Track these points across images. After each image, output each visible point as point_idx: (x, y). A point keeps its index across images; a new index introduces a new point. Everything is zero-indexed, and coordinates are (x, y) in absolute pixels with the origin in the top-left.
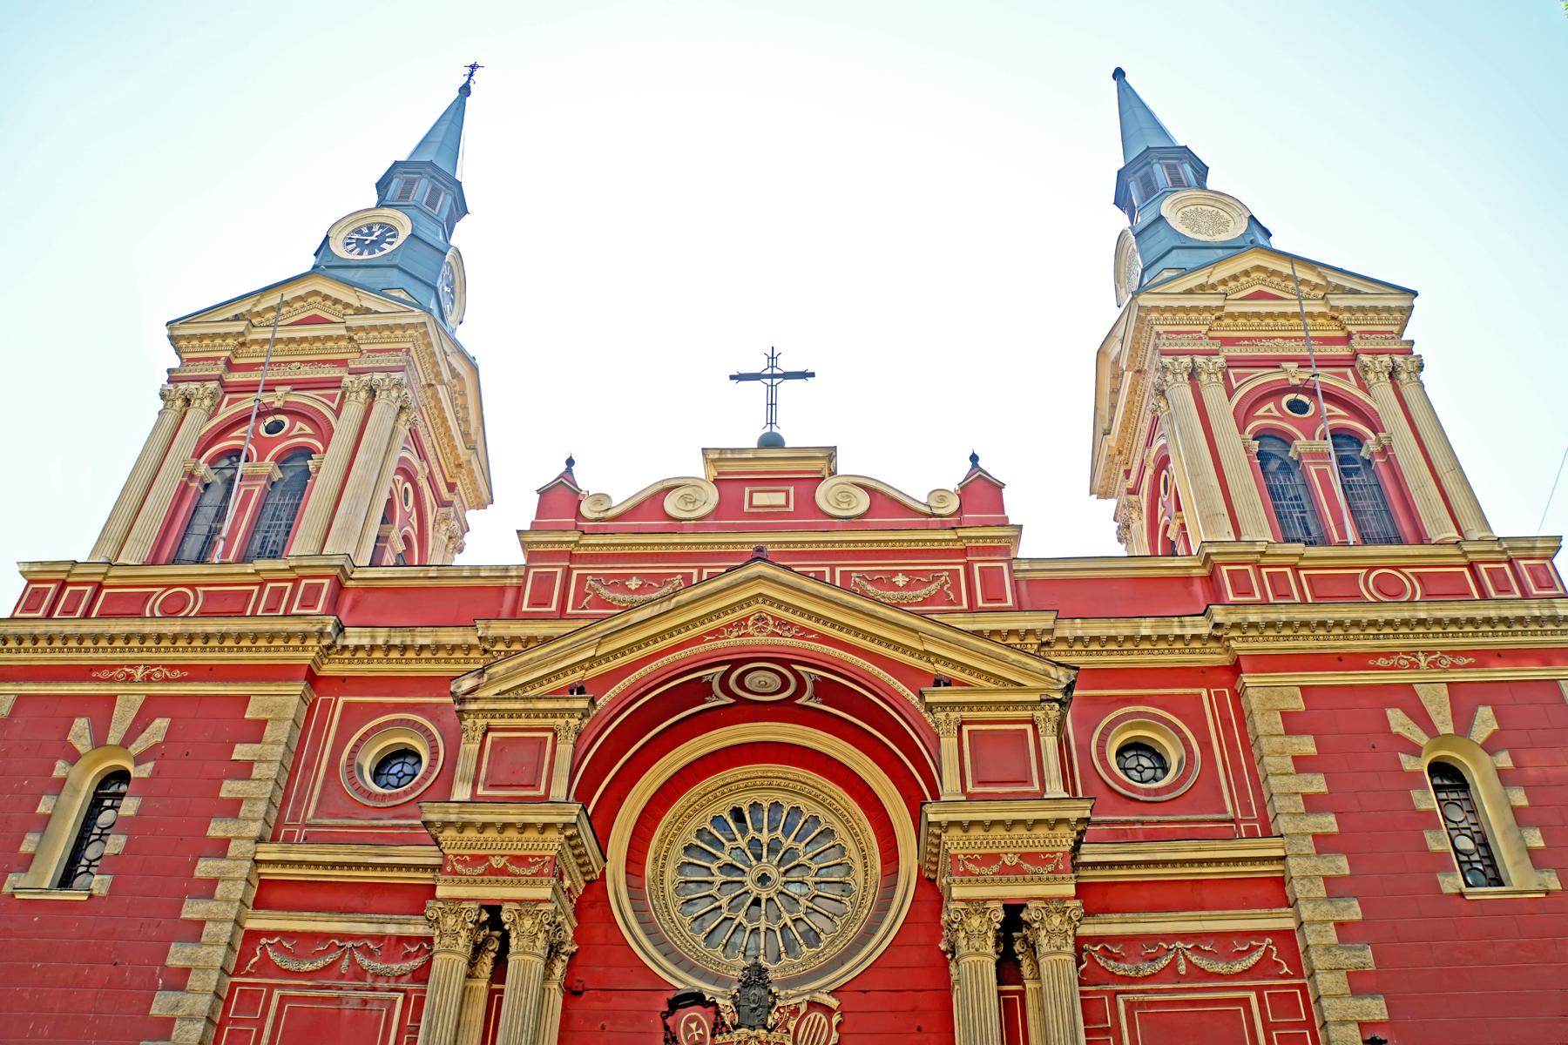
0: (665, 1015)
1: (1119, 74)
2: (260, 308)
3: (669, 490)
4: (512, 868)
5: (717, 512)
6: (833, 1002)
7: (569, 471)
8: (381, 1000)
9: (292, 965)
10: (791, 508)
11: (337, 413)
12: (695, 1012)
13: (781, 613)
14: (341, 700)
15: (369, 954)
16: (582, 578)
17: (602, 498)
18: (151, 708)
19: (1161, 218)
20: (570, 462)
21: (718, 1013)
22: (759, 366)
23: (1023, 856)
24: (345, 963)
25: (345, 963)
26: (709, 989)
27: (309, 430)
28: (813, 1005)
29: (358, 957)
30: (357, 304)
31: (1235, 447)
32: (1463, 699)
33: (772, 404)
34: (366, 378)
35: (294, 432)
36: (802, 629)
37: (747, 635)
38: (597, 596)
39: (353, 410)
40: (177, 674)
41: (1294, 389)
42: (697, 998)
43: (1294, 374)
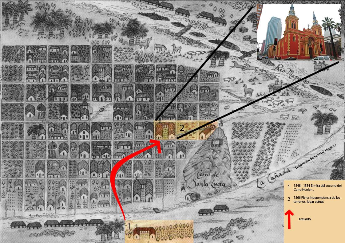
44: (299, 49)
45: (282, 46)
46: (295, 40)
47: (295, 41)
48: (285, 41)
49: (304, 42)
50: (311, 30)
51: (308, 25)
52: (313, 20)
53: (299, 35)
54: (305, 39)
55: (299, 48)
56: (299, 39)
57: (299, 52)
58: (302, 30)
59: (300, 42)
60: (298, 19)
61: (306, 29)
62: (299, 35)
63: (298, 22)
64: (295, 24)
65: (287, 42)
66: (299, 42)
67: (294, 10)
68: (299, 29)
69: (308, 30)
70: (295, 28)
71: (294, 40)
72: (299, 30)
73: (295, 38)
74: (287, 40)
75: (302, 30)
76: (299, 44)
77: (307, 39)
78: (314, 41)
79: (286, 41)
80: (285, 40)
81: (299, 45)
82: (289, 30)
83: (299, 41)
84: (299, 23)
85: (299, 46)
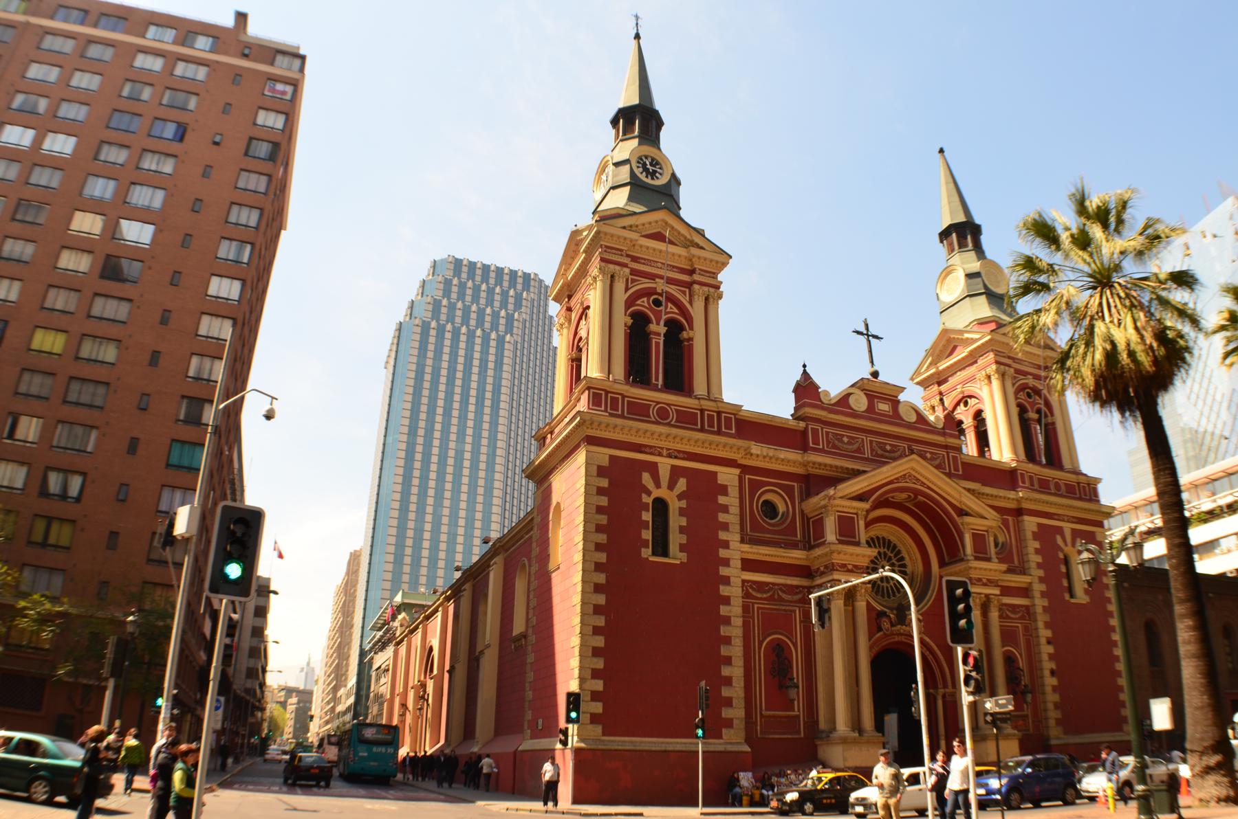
0: (876, 619)
3: (851, 394)
5: (866, 411)
7: (805, 372)
8: (791, 611)
9: (759, 595)
10: (891, 414)
11: (691, 302)
12: (884, 619)
14: (747, 476)
15: (784, 592)
16: (827, 433)
17: (827, 393)
18: (676, 472)
20: (804, 366)
21: (890, 619)
22: (863, 330)
23: (988, 580)
24: (776, 596)
25: (776, 596)
27: (676, 311)
30: (688, 237)
33: (870, 351)
34: (706, 289)
35: (668, 310)
36: (922, 482)
37: (907, 482)
39: (699, 304)
40: (681, 455)
43: (1031, 381)
44: (735, 671)
45: (518, 627)
46: (676, 540)
49: (806, 571)
51: (867, 334)
55: (735, 650)
57: (736, 713)
58: (781, 406)
61: (832, 384)
64: (674, 328)
68: (730, 395)
69: (859, 402)
70: (679, 379)
71: (661, 546)
73: (676, 521)
75: (781, 406)
76: (734, 591)
81: (734, 610)
84: (725, 309)
85: (734, 630)
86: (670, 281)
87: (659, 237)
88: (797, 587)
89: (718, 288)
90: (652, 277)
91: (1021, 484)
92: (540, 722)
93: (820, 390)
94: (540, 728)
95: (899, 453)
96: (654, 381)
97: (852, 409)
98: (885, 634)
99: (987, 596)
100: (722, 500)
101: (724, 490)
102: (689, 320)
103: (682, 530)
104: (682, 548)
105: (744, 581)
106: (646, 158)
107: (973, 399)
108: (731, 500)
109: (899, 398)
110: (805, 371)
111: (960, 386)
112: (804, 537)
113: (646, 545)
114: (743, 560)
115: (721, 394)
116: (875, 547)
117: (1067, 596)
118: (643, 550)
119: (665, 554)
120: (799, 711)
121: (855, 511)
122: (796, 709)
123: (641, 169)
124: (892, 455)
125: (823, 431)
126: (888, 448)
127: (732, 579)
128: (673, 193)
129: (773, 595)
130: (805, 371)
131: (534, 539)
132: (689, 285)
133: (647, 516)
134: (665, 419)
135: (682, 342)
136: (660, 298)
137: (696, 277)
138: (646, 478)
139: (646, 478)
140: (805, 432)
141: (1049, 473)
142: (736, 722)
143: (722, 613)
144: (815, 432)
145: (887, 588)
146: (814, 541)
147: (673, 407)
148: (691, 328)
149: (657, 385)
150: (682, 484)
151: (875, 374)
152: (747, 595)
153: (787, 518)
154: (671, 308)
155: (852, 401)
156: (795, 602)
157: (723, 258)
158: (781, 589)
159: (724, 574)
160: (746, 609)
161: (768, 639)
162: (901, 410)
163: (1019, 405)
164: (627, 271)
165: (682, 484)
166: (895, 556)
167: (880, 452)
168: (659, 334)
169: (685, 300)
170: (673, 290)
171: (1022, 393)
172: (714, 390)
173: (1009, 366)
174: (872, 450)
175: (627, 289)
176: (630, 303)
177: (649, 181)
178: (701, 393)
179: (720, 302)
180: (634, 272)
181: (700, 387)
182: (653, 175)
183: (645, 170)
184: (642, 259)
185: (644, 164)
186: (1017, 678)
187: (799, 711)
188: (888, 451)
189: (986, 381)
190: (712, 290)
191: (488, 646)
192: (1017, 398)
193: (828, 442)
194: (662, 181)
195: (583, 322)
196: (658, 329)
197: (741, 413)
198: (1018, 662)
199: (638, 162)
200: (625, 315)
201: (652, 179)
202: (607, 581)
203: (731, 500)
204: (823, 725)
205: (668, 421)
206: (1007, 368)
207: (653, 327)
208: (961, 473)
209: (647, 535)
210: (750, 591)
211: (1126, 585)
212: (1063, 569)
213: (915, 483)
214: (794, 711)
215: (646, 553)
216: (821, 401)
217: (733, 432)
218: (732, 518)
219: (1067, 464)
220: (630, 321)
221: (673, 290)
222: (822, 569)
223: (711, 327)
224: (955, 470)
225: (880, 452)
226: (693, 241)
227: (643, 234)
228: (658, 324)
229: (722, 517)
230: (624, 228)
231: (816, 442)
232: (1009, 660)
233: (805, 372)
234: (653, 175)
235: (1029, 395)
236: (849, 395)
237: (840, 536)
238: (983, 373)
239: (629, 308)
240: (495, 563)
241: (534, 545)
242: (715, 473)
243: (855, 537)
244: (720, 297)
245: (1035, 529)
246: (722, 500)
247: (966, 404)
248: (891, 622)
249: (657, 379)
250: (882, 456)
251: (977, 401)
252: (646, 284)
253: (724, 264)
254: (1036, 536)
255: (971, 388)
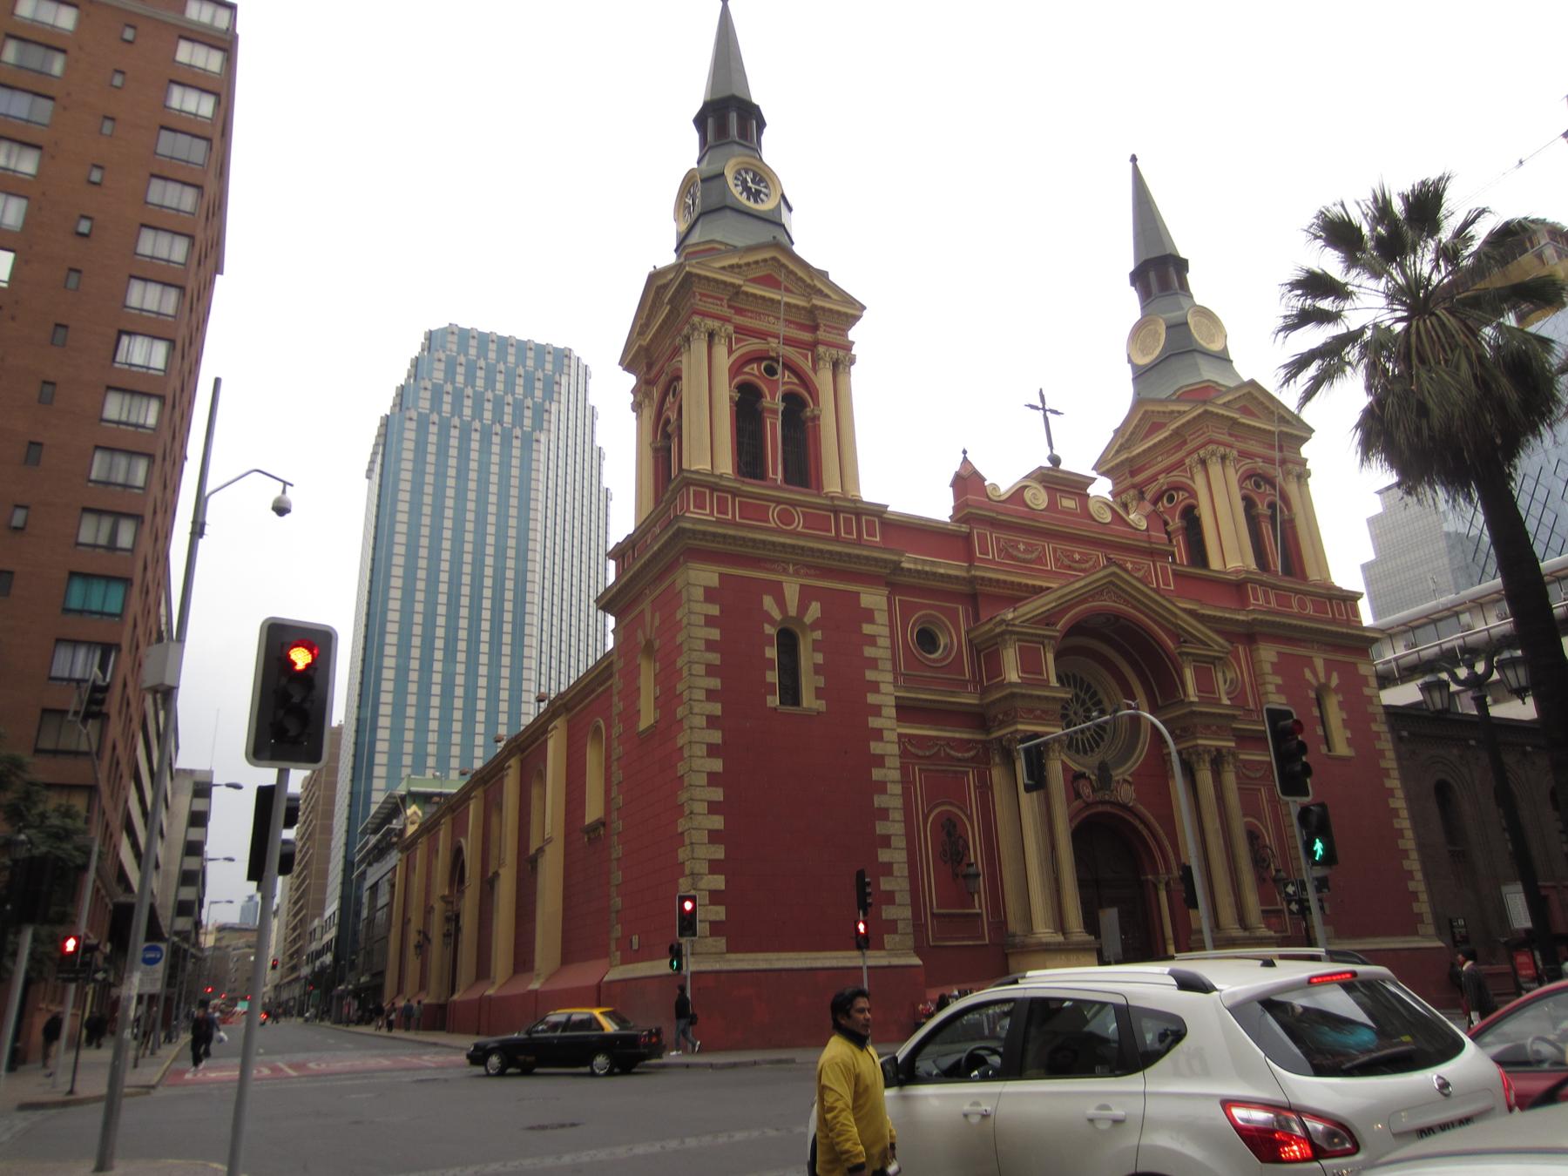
0: (1072, 783)
1: (1134, 159)
2: (742, 262)
4: (1044, 716)
6: (1130, 779)
7: (965, 459)
9: (920, 753)
13: (1117, 591)
17: (995, 487)
18: (806, 595)
19: (1186, 323)
20: (965, 452)
24: (942, 754)
25: (942, 754)
26: (1088, 773)
27: (796, 381)
28: (1125, 781)
29: (948, 750)
30: (809, 281)
31: (1239, 506)
32: (1330, 666)
34: (834, 351)
35: (786, 379)
37: (1105, 600)
38: (1007, 552)
40: (812, 572)
41: (1259, 475)
42: (1082, 776)
44: (895, 856)
45: (593, 811)
46: (809, 684)
47: (809, 700)
48: (632, 715)
50: (1102, 488)
51: (1043, 408)
52: (1129, 307)
53: (873, 598)
54: (986, 654)
55: (894, 828)
56: (884, 678)
57: (899, 912)
58: (938, 506)
59: (906, 711)
60: (849, 311)
62: (873, 598)
63: (842, 361)
65: (668, 725)
66: (887, 721)
67: (774, 149)
71: (791, 692)
72: (878, 512)
73: (808, 658)
74: (668, 700)
75: (938, 506)
76: (888, 748)
77: (1030, 663)
78: (1163, 690)
79: (647, 717)
80: (632, 694)
82: (699, 515)
83: (886, 696)
84: (859, 377)
85: (891, 800)
86: (789, 341)
87: (769, 281)
88: (969, 741)
89: (850, 349)
90: (762, 335)
91: (1252, 601)
92: (635, 939)
93: (986, 483)
94: (635, 946)
95: (1091, 563)
96: (771, 475)
97: (1028, 506)
98: (1084, 801)
99: (1218, 750)
100: (867, 629)
101: (869, 616)
102: (814, 393)
103: (818, 669)
104: (819, 693)
105: (900, 736)
106: (747, 172)
107: (1181, 493)
108: (878, 628)
109: (1089, 491)
110: (965, 458)
111: (1163, 475)
112: (974, 673)
113: (770, 688)
114: (898, 707)
115: (859, 491)
116: (1069, 685)
117: (1324, 749)
118: (768, 697)
119: (796, 701)
120: (980, 907)
121: (1041, 640)
122: (977, 905)
123: (740, 189)
124: (1084, 566)
125: (992, 536)
126: (1077, 557)
127: (886, 734)
128: (784, 220)
129: (939, 750)
130: (965, 458)
131: (615, 691)
132: (813, 346)
133: (772, 653)
134: (789, 525)
135: (804, 423)
136: (775, 365)
137: (821, 334)
138: (768, 602)
139: (768, 602)
140: (968, 538)
141: (1287, 583)
142: (901, 925)
143: (874, 777)
144: (982, 538)
145: (1082, 739)
146: (988, 680)
147: (798, 509)
148: (816, 402)
149: (776, 480)
150: (815, 609)
151: (1055, 461)
152: (904, 754)
153: (952, 648)
154: (789, 377)
155: (1028, 495)
156: (966, 760)
157: (849, 311)
158: (948, 744)
159: (875, 726)
160: (904, 769)
161: (936, 811)
162: (1093, 507)
163: (1245, 498)
164: (730, 328)
165: (815, 609)
166: (1091, 698)
167: (1066, 562)
168: (775, 412)
169: (807, 365)
170: (791, 352)
171: (1248, 482)
172: (848, 487)
173: (1231, 446)
174: (1057, 560)
175: (730, 352)
176: (735, 370)
177: (751, 204)
178: (832, 490)
179: (853, 368)
180: (739, 329)
181: (832, 486)
182: (756, 196)
183: (747, 189)
184: (748, 311)
185: (744, 182)
186: (1264, 860)
187: (980, 907)
188: (1076, 562)
189: (1199, 466)
190: (841, 353)
191: (550, 841)
192: (1241, 488)
193: (1000, 551)
194: (766, 206)
195: (670, 398)
196: (773, 402)
197: (885, 516)
198: (1264, 837)
199: (736, 178)
200: (730, 386)
201: (756, 201)
202: (724, 741)
203: (878, 628)
204: (1014, 925)
205: (792, 527)
206: (1228, 450)
207: (767, 402)
208: (1172, 588)
209: (773, 677)
210: (909, 747)
211: (1405, 734)
212: (1316, 713)
213: (1116, 602)
214: (974, 907)
215: (774, 701)
216: (988, 497)
217: (878, 539)
218: (881, 651)
219: (1313, 575)
220: (737, 396)
221: (791, 352)
222: (1000, 717)
223: (842, 403)
224: (1164, 585)
225: (1066, 562)
226: (815, 286)
227: (750, 277)
228: (773, 397)
229: (869, 652)
230: (723, 268)
231: (984, 551)
232: (1253, 836)
233: (965, 459)
234: (756, 196)
235: (1258, 485)
236: (1025, 487)
237: (1024, 671)
238: (1196, 456)
239: (734, 379)
240: (555, 727)
241: (615, 699)
242: (858, 594)
243: (1042, 674)
244: (852, 361)
245: (1275, 660)
246: (867, 629)
247: (1171, 499)
248: (1093, 787)
249: (775, 472)
250: (1070, 568)
251: (1186, 495)
252: (754, 345)
253: (856, 318)
254: (1277, 669)
255: (1176, 477)
